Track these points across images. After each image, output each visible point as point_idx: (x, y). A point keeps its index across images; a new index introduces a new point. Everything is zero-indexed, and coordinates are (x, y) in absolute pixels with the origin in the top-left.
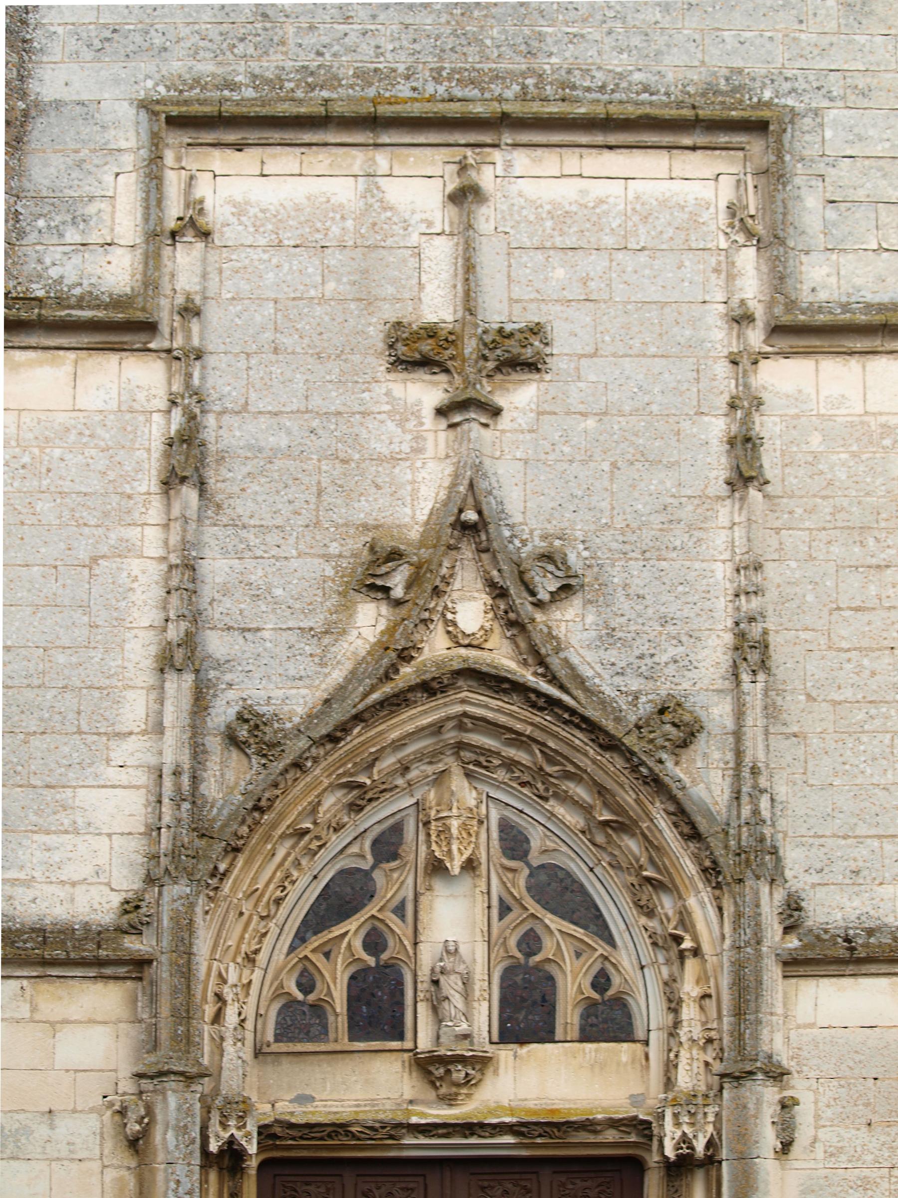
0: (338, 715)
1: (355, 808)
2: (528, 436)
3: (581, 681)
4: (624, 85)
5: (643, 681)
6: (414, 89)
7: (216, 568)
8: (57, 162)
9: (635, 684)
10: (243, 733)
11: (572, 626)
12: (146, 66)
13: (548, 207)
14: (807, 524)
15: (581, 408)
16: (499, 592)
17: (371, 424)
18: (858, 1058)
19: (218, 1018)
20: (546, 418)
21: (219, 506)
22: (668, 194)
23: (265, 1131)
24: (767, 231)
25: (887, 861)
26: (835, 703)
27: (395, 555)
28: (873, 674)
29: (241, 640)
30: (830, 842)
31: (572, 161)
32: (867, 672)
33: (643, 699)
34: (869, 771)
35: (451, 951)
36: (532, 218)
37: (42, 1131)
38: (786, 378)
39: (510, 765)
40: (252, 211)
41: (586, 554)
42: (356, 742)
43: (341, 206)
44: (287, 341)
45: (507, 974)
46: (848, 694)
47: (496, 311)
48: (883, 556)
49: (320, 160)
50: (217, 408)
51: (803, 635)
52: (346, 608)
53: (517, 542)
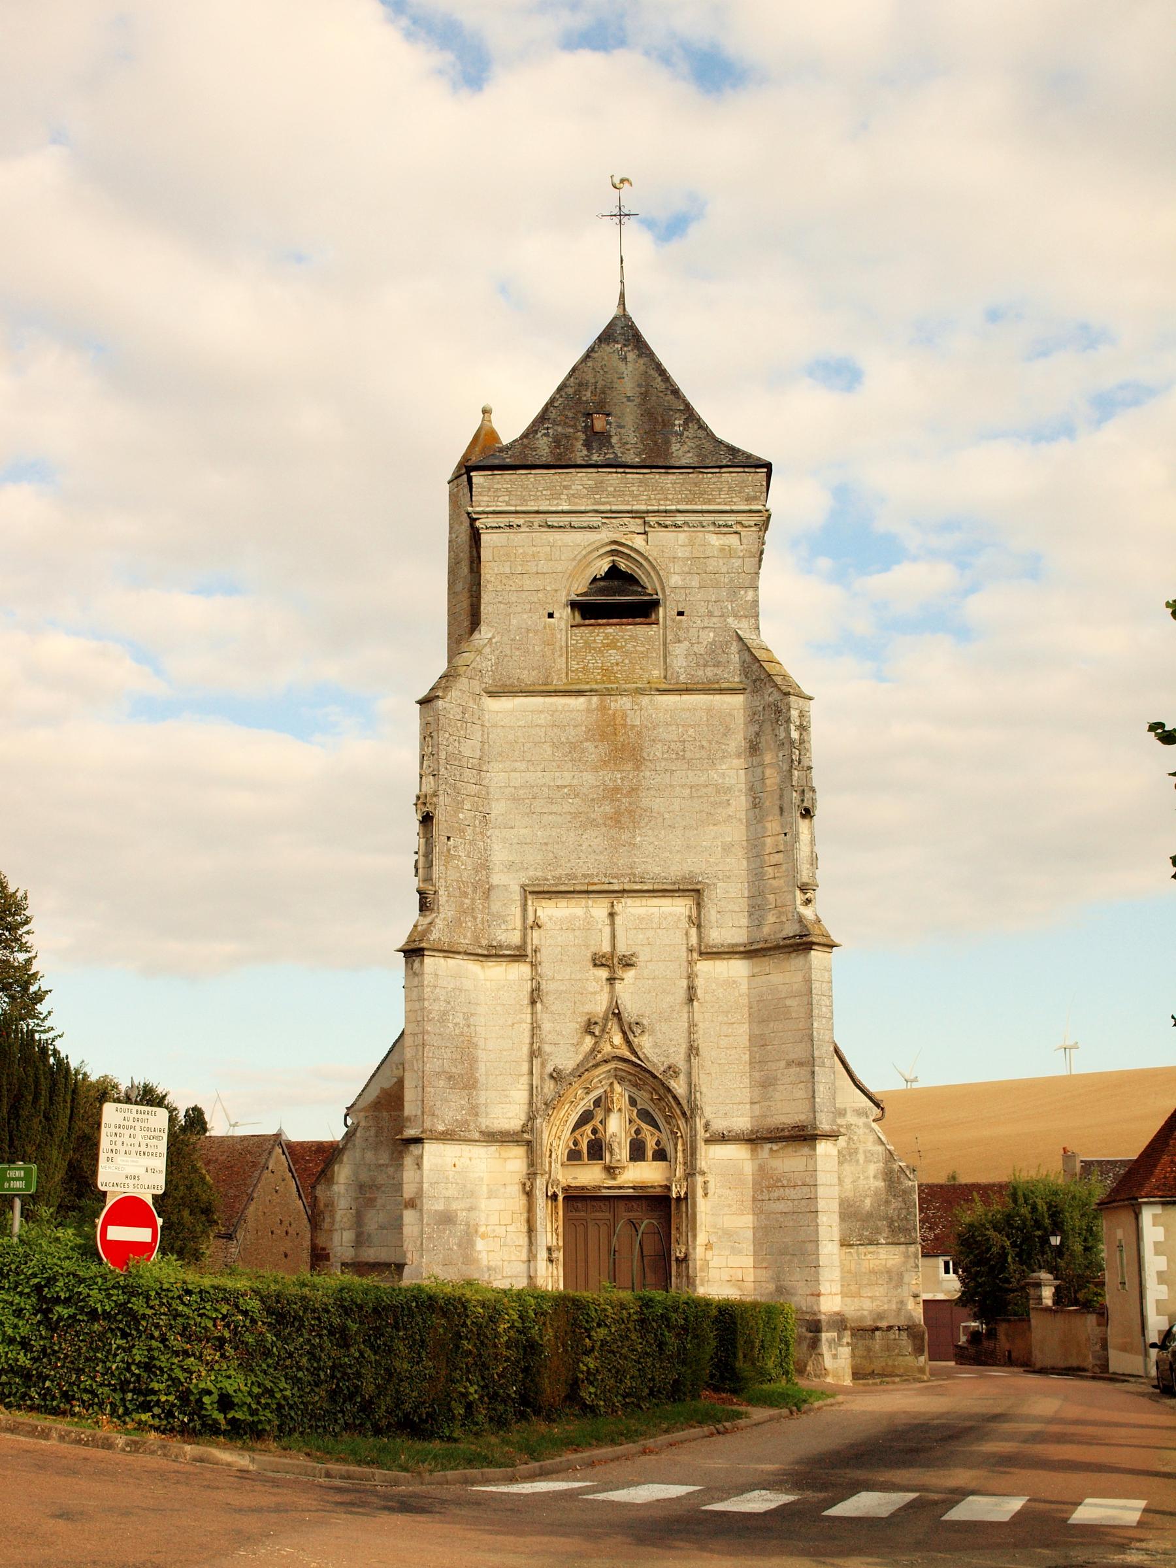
0: (582, 1070)
1: (587, 1093)
3: (647, 1058)
7: (547, 1026)
8: (499, 904)
11: (645, 1044)
12: (522, 874)
16: (624, 1033)
19: (550, 1156)
23: (565, 1189)
24: (697, 923)
27: (596, 1023)
35: (614, 1135)
37: (503, 1190)
38: (704, 967)
44: (565, 958)
47: (622, 949)
52: (583, 1038)
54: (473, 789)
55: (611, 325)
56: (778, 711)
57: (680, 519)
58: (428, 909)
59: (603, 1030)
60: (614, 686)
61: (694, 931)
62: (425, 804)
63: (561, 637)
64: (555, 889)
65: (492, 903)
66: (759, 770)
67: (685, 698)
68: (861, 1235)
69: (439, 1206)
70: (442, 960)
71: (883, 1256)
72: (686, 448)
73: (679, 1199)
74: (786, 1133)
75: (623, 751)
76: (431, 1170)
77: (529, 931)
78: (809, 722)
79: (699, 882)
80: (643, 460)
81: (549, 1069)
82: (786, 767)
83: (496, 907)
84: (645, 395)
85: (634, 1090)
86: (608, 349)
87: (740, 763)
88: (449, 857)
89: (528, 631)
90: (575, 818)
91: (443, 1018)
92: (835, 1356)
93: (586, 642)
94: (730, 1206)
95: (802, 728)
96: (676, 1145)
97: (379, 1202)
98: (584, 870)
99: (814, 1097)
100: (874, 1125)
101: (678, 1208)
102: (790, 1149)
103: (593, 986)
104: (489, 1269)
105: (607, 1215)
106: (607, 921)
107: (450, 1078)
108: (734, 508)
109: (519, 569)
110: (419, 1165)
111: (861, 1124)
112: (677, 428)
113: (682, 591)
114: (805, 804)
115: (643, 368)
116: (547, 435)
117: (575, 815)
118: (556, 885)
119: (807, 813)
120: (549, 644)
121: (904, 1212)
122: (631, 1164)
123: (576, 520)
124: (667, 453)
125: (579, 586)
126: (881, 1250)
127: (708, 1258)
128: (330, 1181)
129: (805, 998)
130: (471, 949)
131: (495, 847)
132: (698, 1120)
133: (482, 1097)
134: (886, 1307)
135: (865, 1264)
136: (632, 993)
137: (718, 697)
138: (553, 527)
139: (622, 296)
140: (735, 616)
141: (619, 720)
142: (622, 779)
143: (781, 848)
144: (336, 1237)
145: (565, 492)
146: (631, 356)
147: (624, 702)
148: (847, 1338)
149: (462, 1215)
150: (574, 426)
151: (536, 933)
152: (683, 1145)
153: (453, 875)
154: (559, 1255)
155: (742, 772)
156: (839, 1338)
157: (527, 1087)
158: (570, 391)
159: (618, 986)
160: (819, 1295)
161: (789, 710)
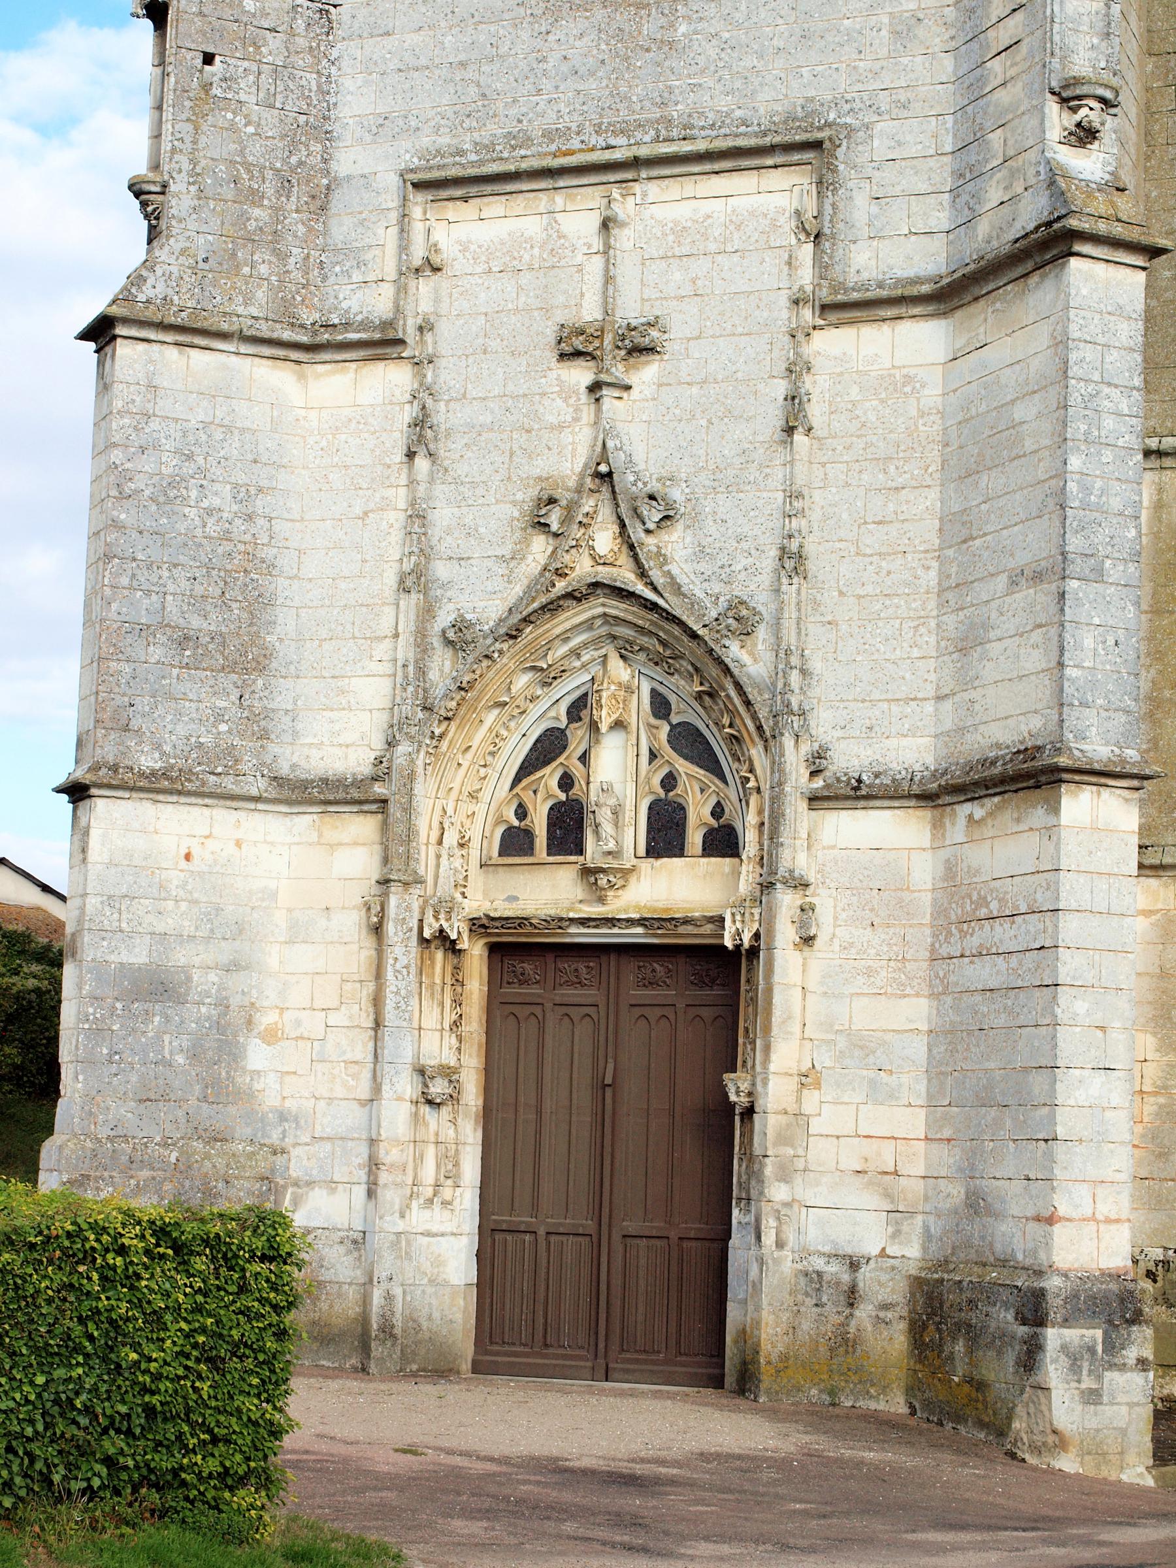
2: (651, 403)
3: (677, 589)
4: (728, 121)
5: (722, 584)
6: (582, 142)
7: (442, 516)
8: (348, 221)
9: (717, 587)
12: (405, 144)
13: (670, 225)
14: (845, 458)
15: (688, 379)
17: (546, 402)
18: (866, 873)
20: (664, 388)
21: (446, 470)
22: (755, 206)
25: (893, 719)
26: (859, 597)
28: (889, 573)
29: (457, 567)
30: (852, 704)
31: (689, 187)
32: (885, 572)
33: (722, 599)
34: (882, 649)
36: (659, 234)
38: (834, 345)
40: (473, 247)
41: (687, 491)
42: (529, 638)
43: (531, 238)
44: (494, 344)
46: (869, 589)
47: (630, 310)
48: (900, 480)
50: (446, 397)
51: (838, 545)
52: (526, 541)
53: (640, 484)
59: (566, 520)
65: (333, 223)
69: (138, 955)
70: (172, 353)
76: (111, 864)
79: (828, 125)
81: (444, 618)
83: (341, 229)
85: (657, 673)
91: (169, 493)
94: (869, 973)
99: (1061, 665)
102: (1008, 815)
103: (556, 410)
104: (283, 1117)
105: (590, 994)
106: (597, 244)
107: (185, 640)
118: (481, 163)
122: (646, 865)
127: (807, 1108)
129: (1053, 394)
130: (264, 330)
131: (348, 84)
132: (788, 741)
133: (283, 695)
136: (648, 423)
149: (205, 981)
152: (760, 812)
160: (1050, 1220)
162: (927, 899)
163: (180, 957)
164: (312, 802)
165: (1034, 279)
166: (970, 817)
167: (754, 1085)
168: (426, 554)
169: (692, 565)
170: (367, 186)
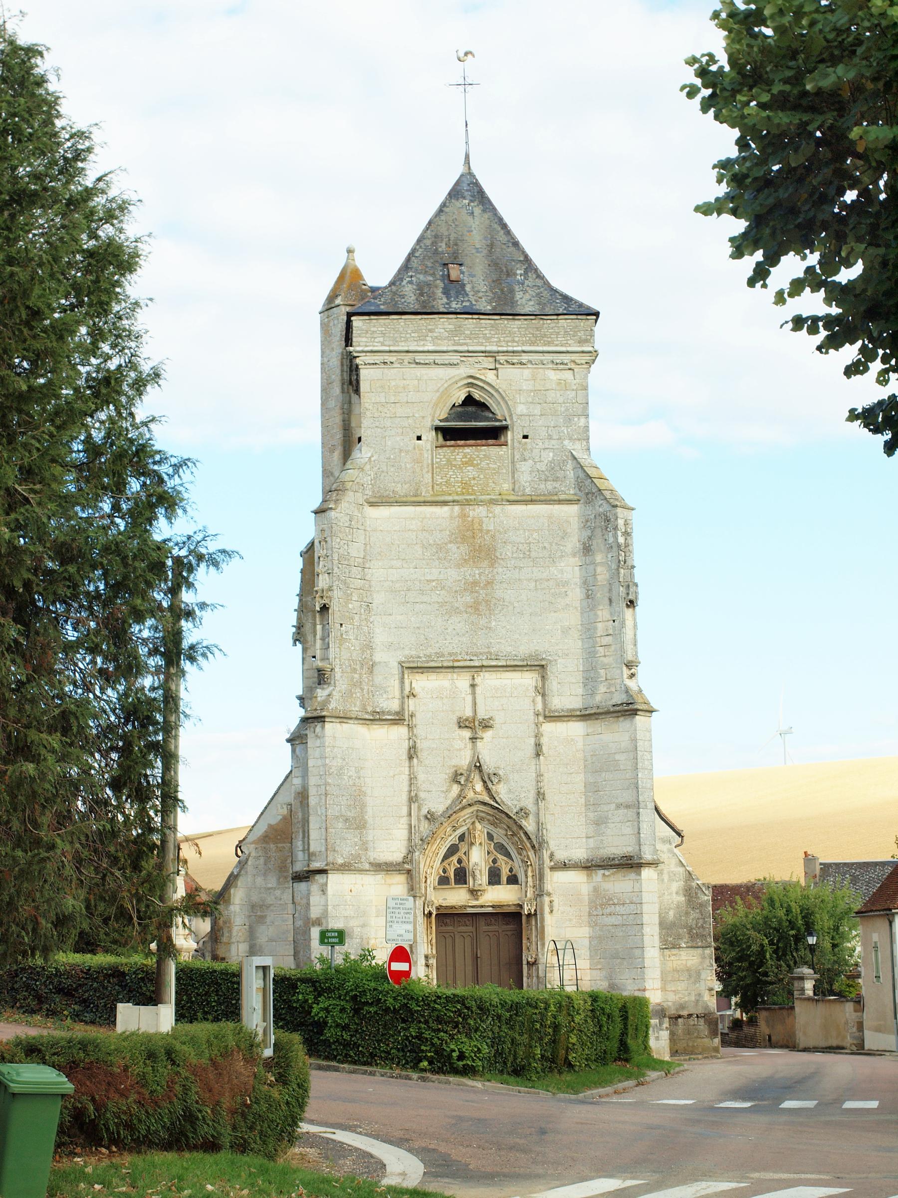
0: (450, 812)
1: (454, 830)
7: (421, 777)
9: (516, 803)
10: (429, 816)
11: (502, 791)
16: (484, 782)
19: (426, 882)
23: (437, 909)
24: (543, 693)
27: (461, 774)
31: (499, 675)
35: (476, 864)
38: (548, 728)
39: (489, 820)
45: (490, 868)
47: (482, 714)
49: (441, 676)
52: (451, 786)
54: (359, 583)
55: (457, 183)
56: (608, 520)
57: (525, 358)
58: (325, 683)
59: (467, 780)
60: (472, 497)
61: (539, 699)
62: (322, 597)
63: (427, 455)
64: (426, 665)
66: (592, 567)
67: (530, 507)
68: (666, 941)
70: (338, 725)
71: (683, 958)
72: (527, 296)
73: (529, 915)
74: (617, 862)
75: (480, 551)
77: (406, 700)
78: (632, 528)
79: (543, 659)
80: (494, 308)
81: (424, 811)
82: (614, 566)
83: (378, 679)
84: (491, 246)
85: (491, 827)
86: (458, 204)
87: (577, 560)
88: (342, 640)
89: (401, 451)
90: (441, 606)
92: (657, 1038)
93: (448, 460)
94: (570, 920)
95: (627, 534)
96: (526, 871)
97: (268, 920)
98: (450, 649)
99: (639, 833)
100: (676, 851)
101: (528, 922)
103: (458, 744)
105: (470, 928)
106: (469, 690)
108: (569, 349)
109: (392, 399)
110: (324, 891)
111: (665, 850)
112: (518, 277)
113: (527, 418)
114: (630, 597)
115: (487, 222)
116: (410, 282)
117: (442, 604)
118: (428, 662)
119: (631, 604)
120: (418, 461)
121: (701, 921)
122: (490, 887)
123: (438, 358)
124: (513, 303)
125: (441, 414)
126: (682, 953)
128: (228, 902)
131: (377, 630)
132: (545, 851)
133: (370, 835)
134: (686, 999)
135: (670, 964)
136: (490, 748)
137: (557, 507)
138: (420, 364)
139: (467, 157)
140: (570, 439)
141: (476, 526)
142: (480, 574)
143: (611, 632)
144: (233, 948)
145: (430, 334)
146: (477, 211)
147: (481, 511)
148: (666, 1024)
149: (357, 931)
150: (433, 274)
151: (412, 701)
152: (532, 871)
153: (345, 655)
154: (433, 961)
155: (577, 569)
156: (661, 1024)
157: (407, 827)
158: (428, 242)
159: (479, 744)
161: (616, 519)
162: (586, 898)
163: (352, 923)
164: (383, 870)
165: (621, 719)
166: (604, 874)
167: (537, 955)
168: (418, 789)
169: (509, 795)
170: (387, 666)
